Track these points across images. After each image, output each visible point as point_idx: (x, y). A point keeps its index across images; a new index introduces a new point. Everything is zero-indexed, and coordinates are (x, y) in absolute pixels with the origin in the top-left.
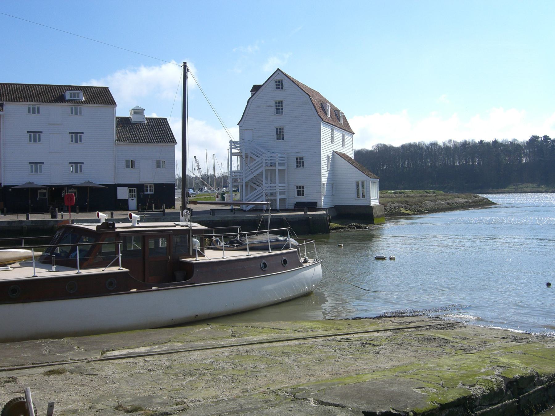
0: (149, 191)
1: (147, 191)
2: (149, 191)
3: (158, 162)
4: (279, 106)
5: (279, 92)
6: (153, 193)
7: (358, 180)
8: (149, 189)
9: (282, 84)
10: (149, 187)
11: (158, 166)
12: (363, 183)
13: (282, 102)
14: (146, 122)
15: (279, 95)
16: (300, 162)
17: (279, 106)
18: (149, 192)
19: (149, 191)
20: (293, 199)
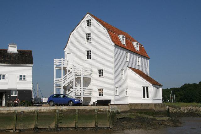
0: (14, 94)
1: (13, 94)
2: (14, 95)
3: (21, 76)
4: (89, 36)
5: (89, 28)
6: (17, 95)
7: (144, 86)
8: (14, 93)
9: (90, 23)
10: (14, 92)
11: (21, 79)
12: (147, 88)
13: (90, 34)
14: (17, 53)
15: (88, 30)
16: (101, 73)
17: (89, 36)
18: (14, 95)
19: (14, 94)
20: (95, 98)
